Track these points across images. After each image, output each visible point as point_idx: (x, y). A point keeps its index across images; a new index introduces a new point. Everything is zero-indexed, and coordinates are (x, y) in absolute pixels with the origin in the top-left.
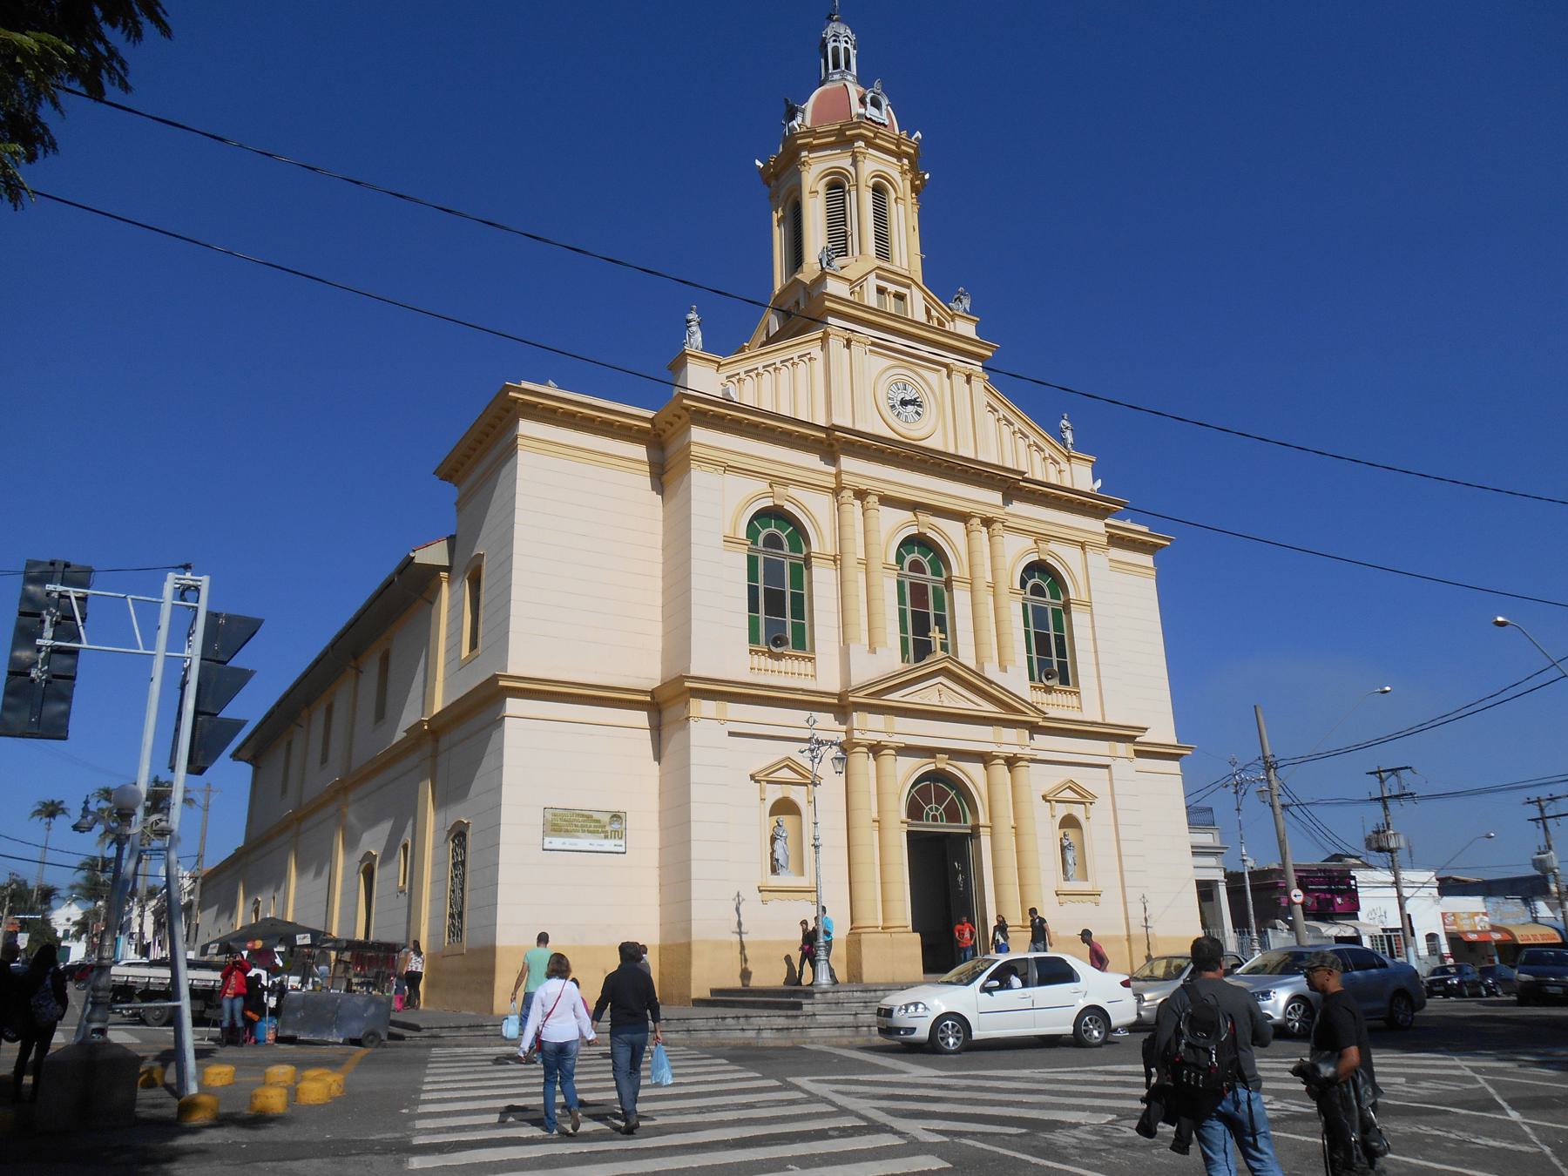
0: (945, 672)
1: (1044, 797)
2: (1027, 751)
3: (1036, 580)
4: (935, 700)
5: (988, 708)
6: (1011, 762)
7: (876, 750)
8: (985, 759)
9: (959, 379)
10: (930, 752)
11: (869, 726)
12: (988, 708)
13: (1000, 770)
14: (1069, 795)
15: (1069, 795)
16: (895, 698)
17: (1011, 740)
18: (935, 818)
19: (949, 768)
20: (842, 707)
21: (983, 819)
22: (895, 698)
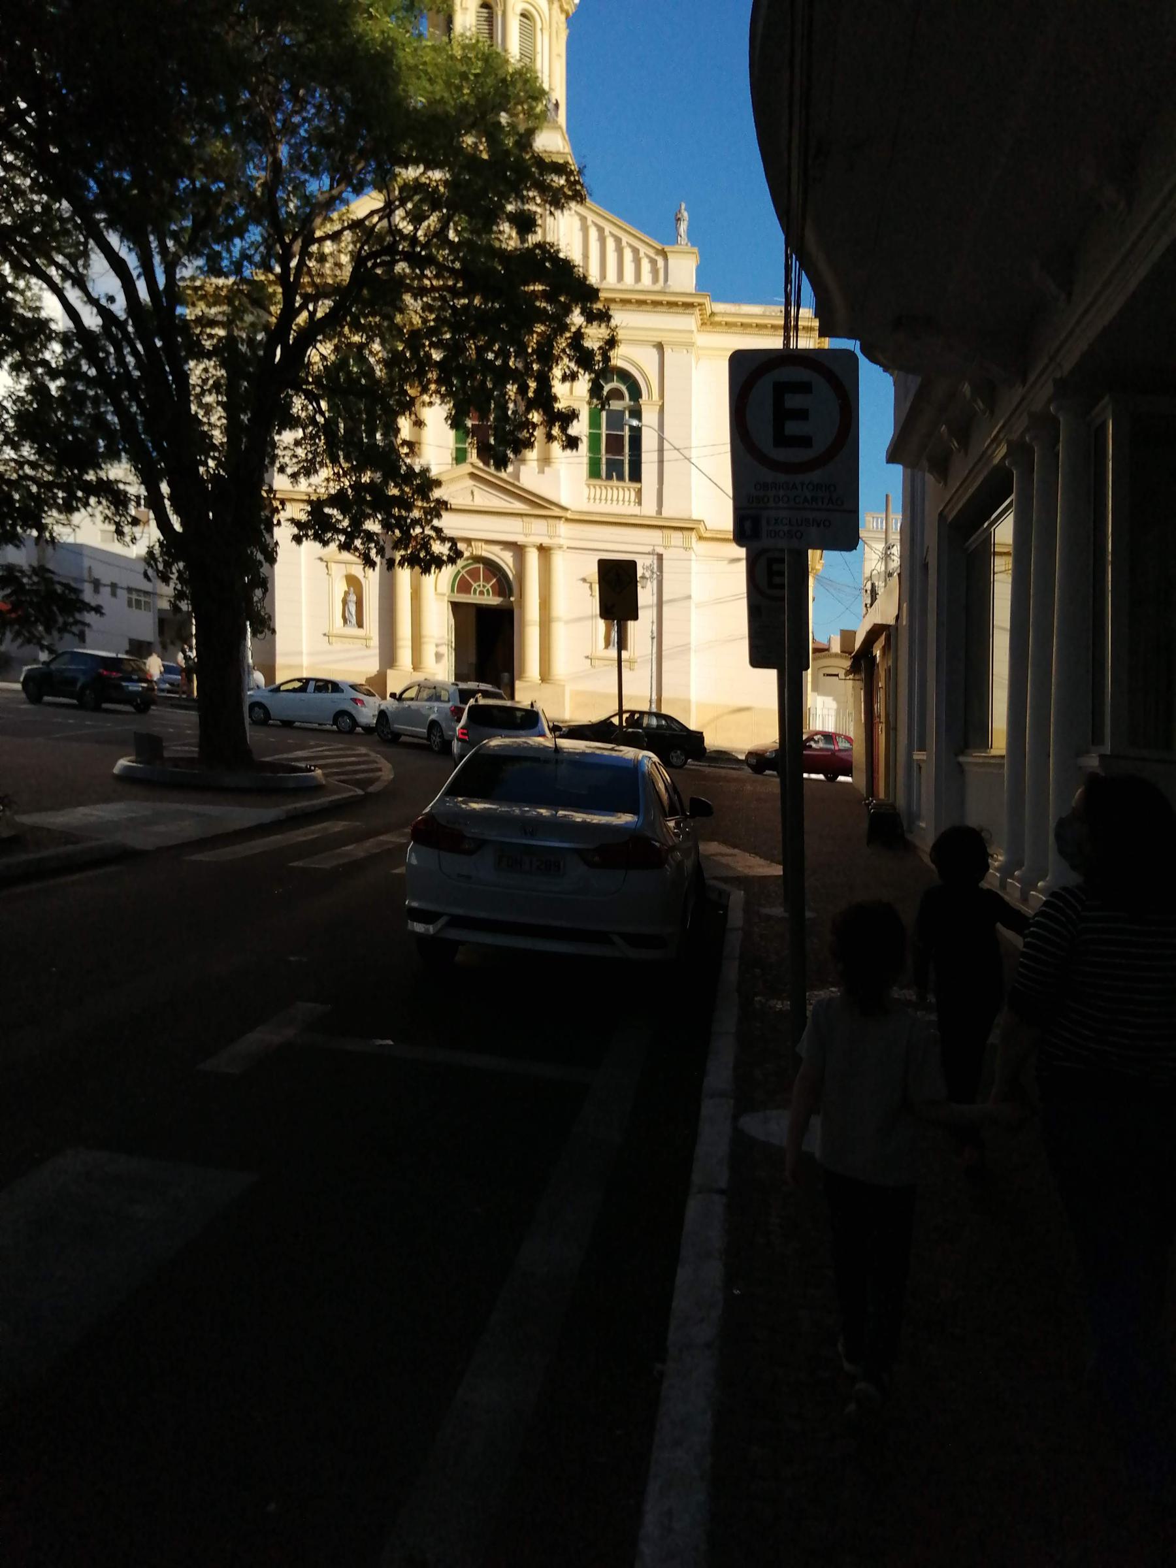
18: (481, 593)
19: (484, 554)
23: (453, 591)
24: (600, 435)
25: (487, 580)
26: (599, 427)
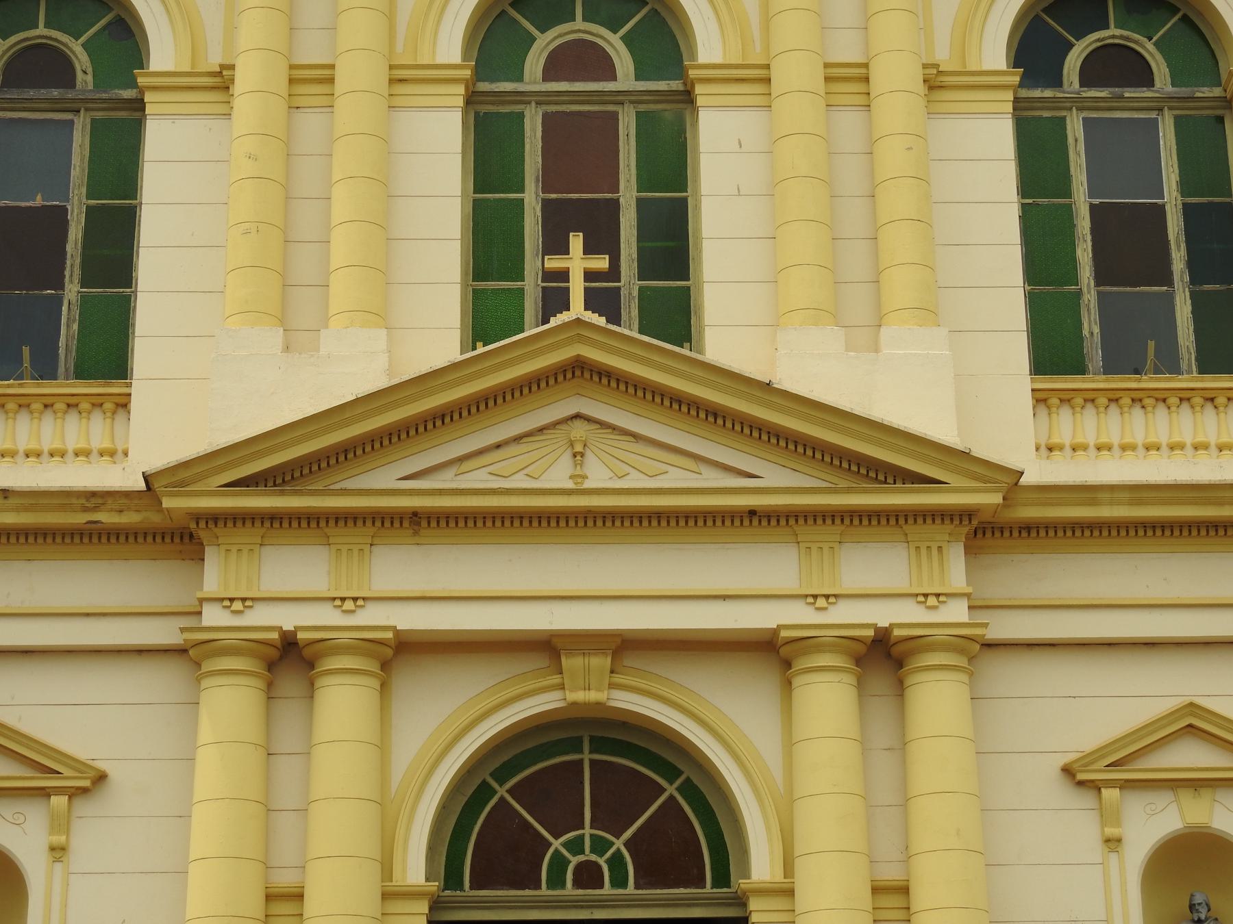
0: (579, 371)
1: (1068, 771)
2: (957, 612)
3: (1112, 33)
4: (558, 475)
5: (778, 481)
6: (883, 658)
7: (290, 660)
8: (774, 653)
10: (548, 648)
11: (290, 586)
12: (778, 481)
13: (827, 697)
14: (1192, 757)
15: (1192, 757)
16: (384, 482)
17: (879, 585)
18: (588, 876)
20: (163, 527)
21: (762, 865)
22: (384, 482)
23: (452, 878)
24: (1068, 213)
25: (612, 816)
26: (1063, 187)
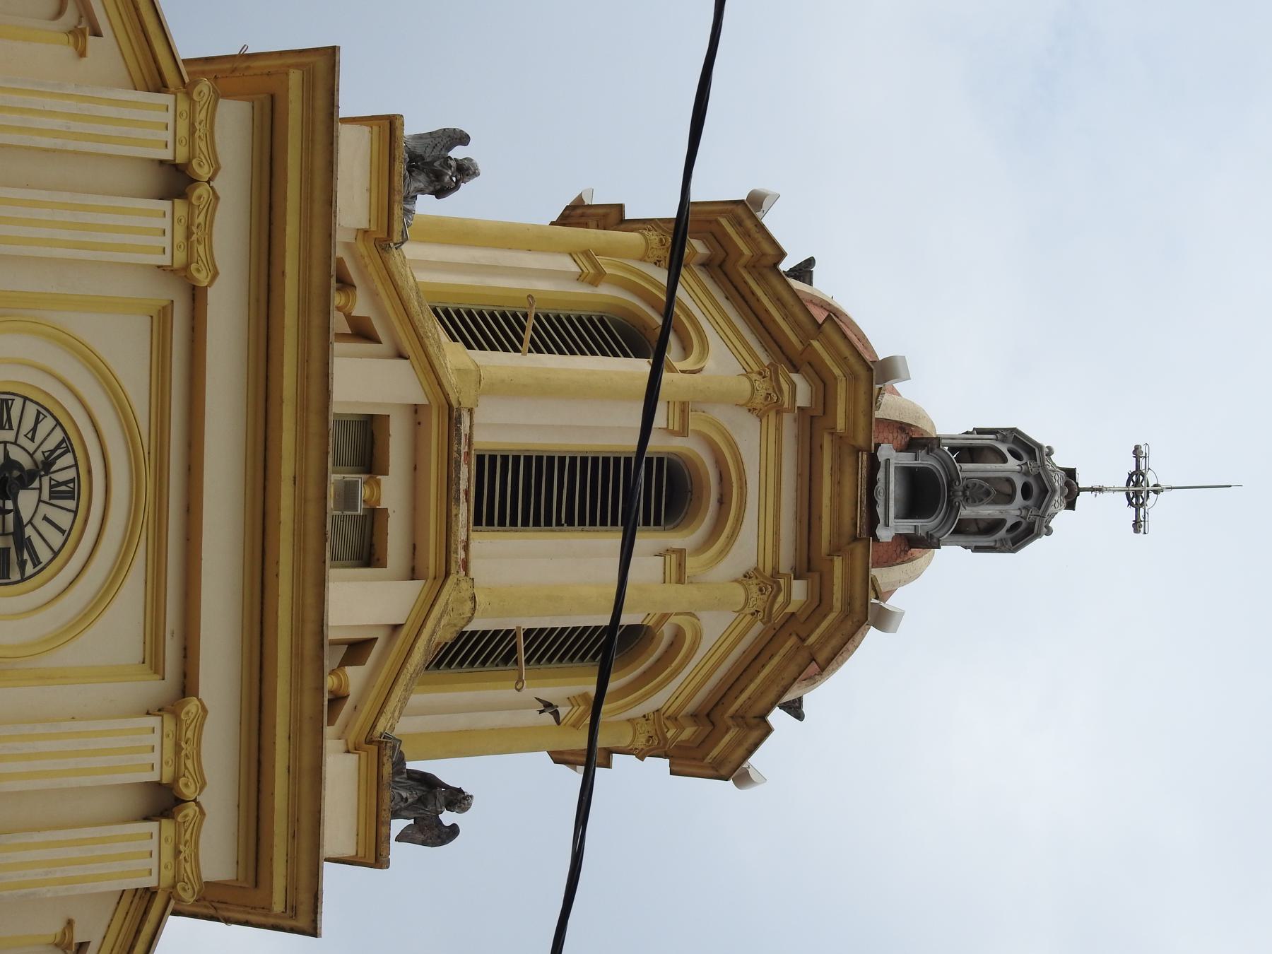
9: (140, 754)
